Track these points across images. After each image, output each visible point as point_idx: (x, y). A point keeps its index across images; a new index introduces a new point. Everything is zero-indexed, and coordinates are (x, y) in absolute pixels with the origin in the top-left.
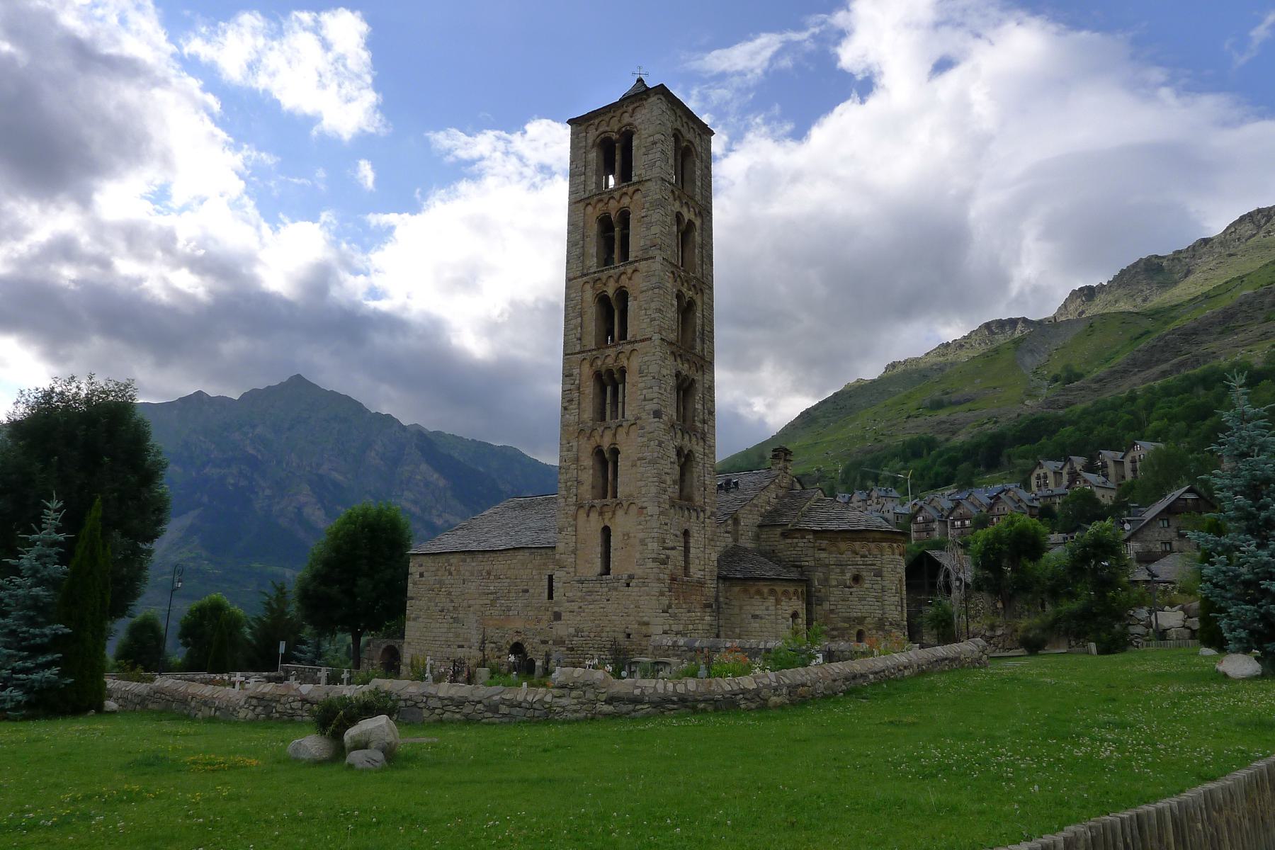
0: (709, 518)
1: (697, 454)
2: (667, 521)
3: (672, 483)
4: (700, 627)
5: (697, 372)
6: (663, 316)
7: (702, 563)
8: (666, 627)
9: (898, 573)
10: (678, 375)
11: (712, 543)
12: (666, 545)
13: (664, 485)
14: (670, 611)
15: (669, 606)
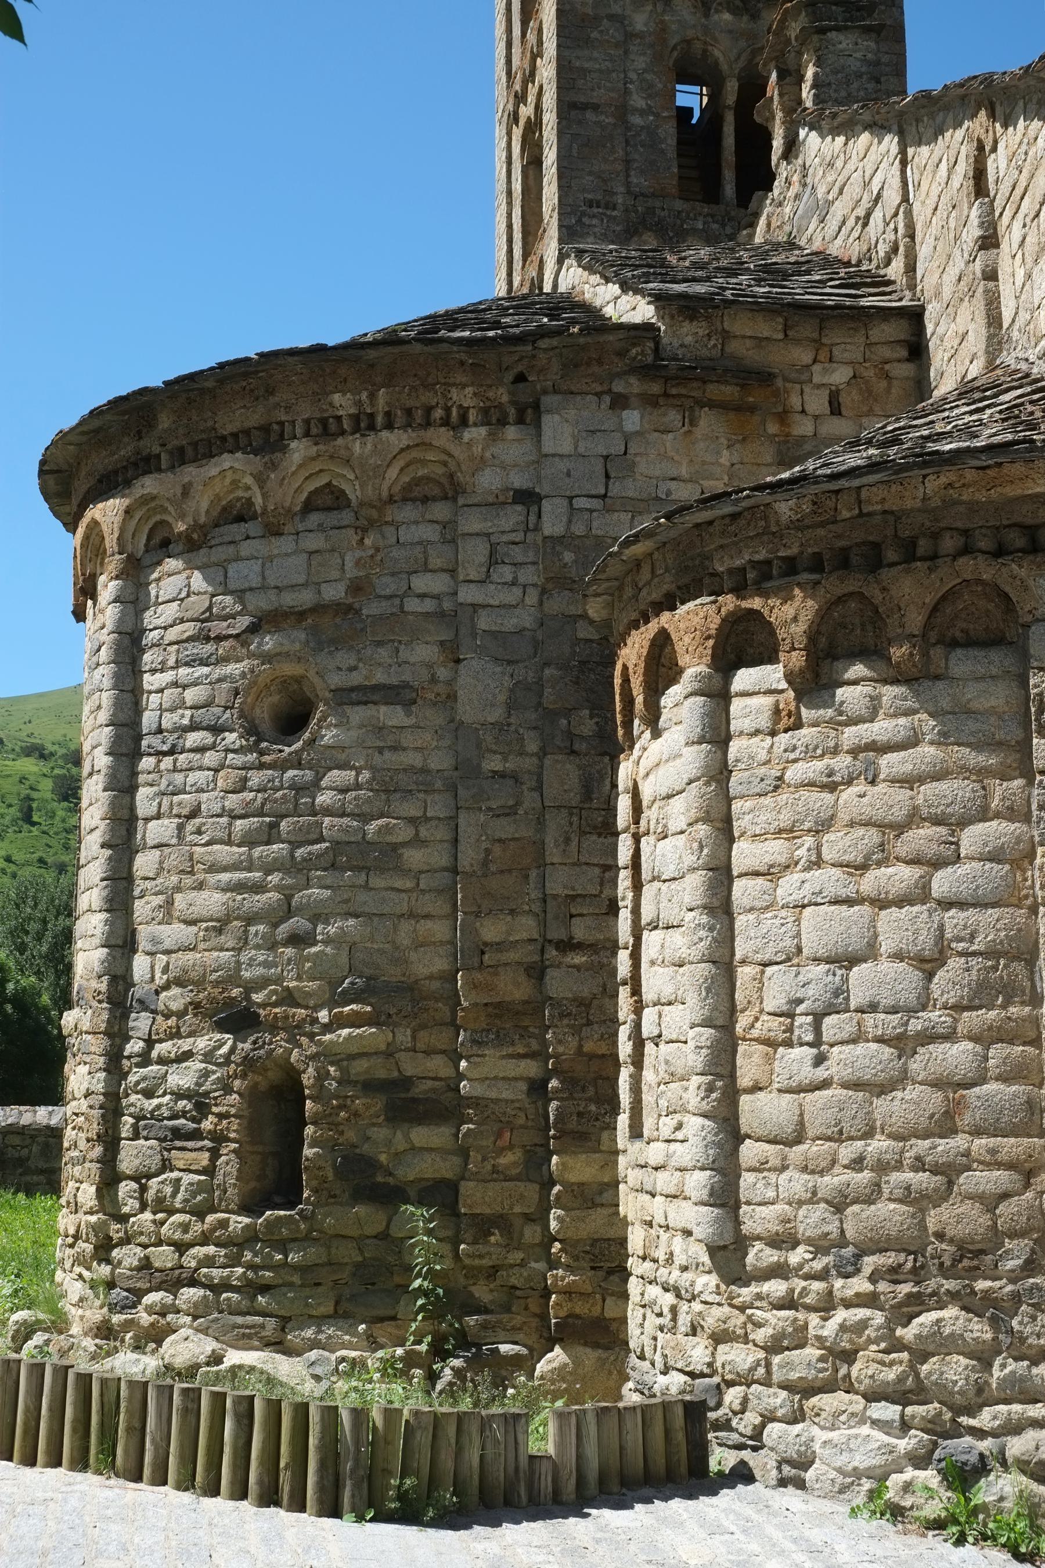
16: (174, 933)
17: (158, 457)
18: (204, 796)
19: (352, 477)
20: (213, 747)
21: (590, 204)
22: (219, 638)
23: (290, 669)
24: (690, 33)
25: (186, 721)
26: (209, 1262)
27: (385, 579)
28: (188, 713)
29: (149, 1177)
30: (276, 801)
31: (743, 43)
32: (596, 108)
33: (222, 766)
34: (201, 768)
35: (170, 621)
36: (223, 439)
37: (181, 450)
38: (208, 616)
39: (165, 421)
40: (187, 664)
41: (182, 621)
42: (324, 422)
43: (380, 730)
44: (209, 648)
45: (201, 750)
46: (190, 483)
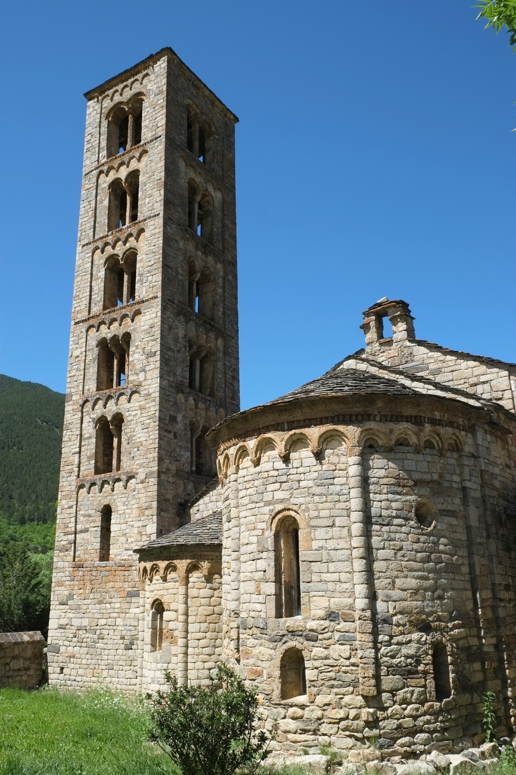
0: (142, 482)
1: (127, 414)
2: (71, 504)
3: (86, 459)
4: (119, 621)
5: (133, 320)
6: (78, 301)
7: (130, 540)
8: (63, 622)
9: (268, 503)
10: (102, 344)
11: (147, 512)
12: (69, 530)
13: (70, 467)
14: (70, 602)
15: (71, 597)
16: (396, 594)
17: (375, 416)
18: (404, 543)
19: (438, 439)
20: (405, 525)
21: (169, 300)
22: (404, 486)
23: (425, 500)
24: (192, 254)
25: (394, 514)
26: (428, 722)
27: (447, 475)
28: (395, 512)
29: (397, 690)
30: (429, 547)
31: (204, 264)
32: (171, 268)
33: (410, 533)
34: (401, 532)
35: (382, 476)
36: (402, 416)
37: (386, 416)
38: (398, 477)
39: (380, 404)
40: (391, 493)
41: (387, 477)
42: (432, 419)
43: (451, 525)
44: (399, 489)
45: (401, 526)
46: (392, 429)
